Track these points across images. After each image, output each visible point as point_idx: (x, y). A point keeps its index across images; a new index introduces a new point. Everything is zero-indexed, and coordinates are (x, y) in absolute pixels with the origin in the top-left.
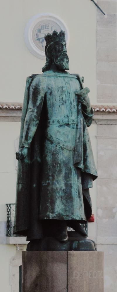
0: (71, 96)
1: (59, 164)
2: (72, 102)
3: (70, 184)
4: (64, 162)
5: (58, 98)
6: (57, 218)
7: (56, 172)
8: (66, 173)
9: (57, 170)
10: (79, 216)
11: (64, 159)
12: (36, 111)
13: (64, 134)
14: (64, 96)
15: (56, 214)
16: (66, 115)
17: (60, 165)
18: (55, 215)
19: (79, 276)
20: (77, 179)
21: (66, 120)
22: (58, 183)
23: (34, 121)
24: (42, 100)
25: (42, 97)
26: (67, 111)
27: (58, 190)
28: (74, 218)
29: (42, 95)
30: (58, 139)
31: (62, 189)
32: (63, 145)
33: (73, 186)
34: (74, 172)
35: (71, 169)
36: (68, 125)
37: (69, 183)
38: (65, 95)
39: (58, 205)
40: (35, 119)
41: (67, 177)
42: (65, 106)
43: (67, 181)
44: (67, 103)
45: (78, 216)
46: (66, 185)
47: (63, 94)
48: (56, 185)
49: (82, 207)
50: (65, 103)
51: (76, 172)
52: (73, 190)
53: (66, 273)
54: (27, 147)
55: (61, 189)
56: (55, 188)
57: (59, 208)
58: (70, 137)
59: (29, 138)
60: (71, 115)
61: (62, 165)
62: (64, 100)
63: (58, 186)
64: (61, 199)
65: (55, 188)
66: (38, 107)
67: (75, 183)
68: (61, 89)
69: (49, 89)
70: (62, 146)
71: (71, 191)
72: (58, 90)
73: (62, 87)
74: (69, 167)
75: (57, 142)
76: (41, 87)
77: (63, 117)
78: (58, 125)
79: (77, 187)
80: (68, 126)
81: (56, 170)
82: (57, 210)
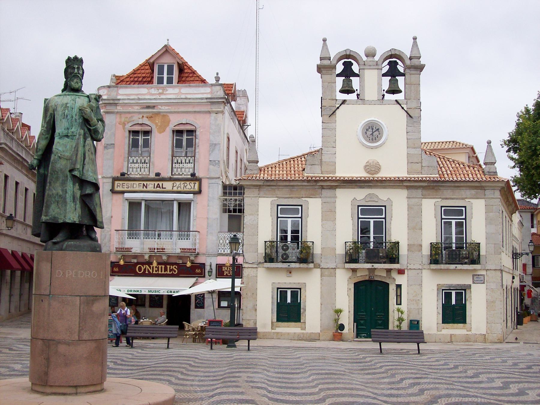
0: (73, 111)
1: (56, 171)
2: (74, 116)
3: (66, 190)
4: (61, 170)
5: (60, 113)
6: (50, 221)
7: (53, 179)
8: (63, 180)
9: (54, 177)
10: (71, 219)
11: (62, 167)
12: (46, 126)
13: (63, 144)
14: (67, 111)
15: (50, 217)
16: (66, 127)
17: (57, 172)
18: (48, 218)
19: (61, 275)
20: (72, 186)
21: (65, 132)
22: (54, 189)
23: (43, 135)
24: (52, 117)
25: (51, 114)
26: (68, 124)
27: (55, 195)
28: (65, 221)
29: (51, 111)
30: (57, 149)
31: (59, 194)
32: (61, 155)
33: (68, 191)
34: (70, 179)
35: (67, 177)
36: (67, 136)
37: (65, 189)
38: (68, 110)
39: (53, 210)
40: (44, 134)
41: (64, 183)
42: (66, 120)
43: (64, 187)
44: (69, 117)
45: (70, 219)
46: (62, 190)
47: (66, 110)
48: (52, 190)
49: (76, 210)
50: (67, 116)
51: (72, 179)
52: (67, 195)
53: (50, 271)
54: (37, 158)
55: (57, 194)
56: (51, 194)
57: (54, 211)
58: (68, 147)
59: (38, 150)
60: (71, 127)
61: (59, 172)
62: (66, 114)
63: (54, 192)
64: (56, 203)
65: (51, 194)
66: (47, 123)
67: (70, 188)
68: (65, 105)
69: (55, 106)
70: (59, 155)
71: (66, 196)
72: (62, 106)
73: (67, 104)
74: (66, 174)
75: (56, 152)
76: (50, 105)
77: (63, 130)
78: (59, 137)
79: (72, 193)
80: (67, 138)
81: (53, 177)
82: (51, 214)
